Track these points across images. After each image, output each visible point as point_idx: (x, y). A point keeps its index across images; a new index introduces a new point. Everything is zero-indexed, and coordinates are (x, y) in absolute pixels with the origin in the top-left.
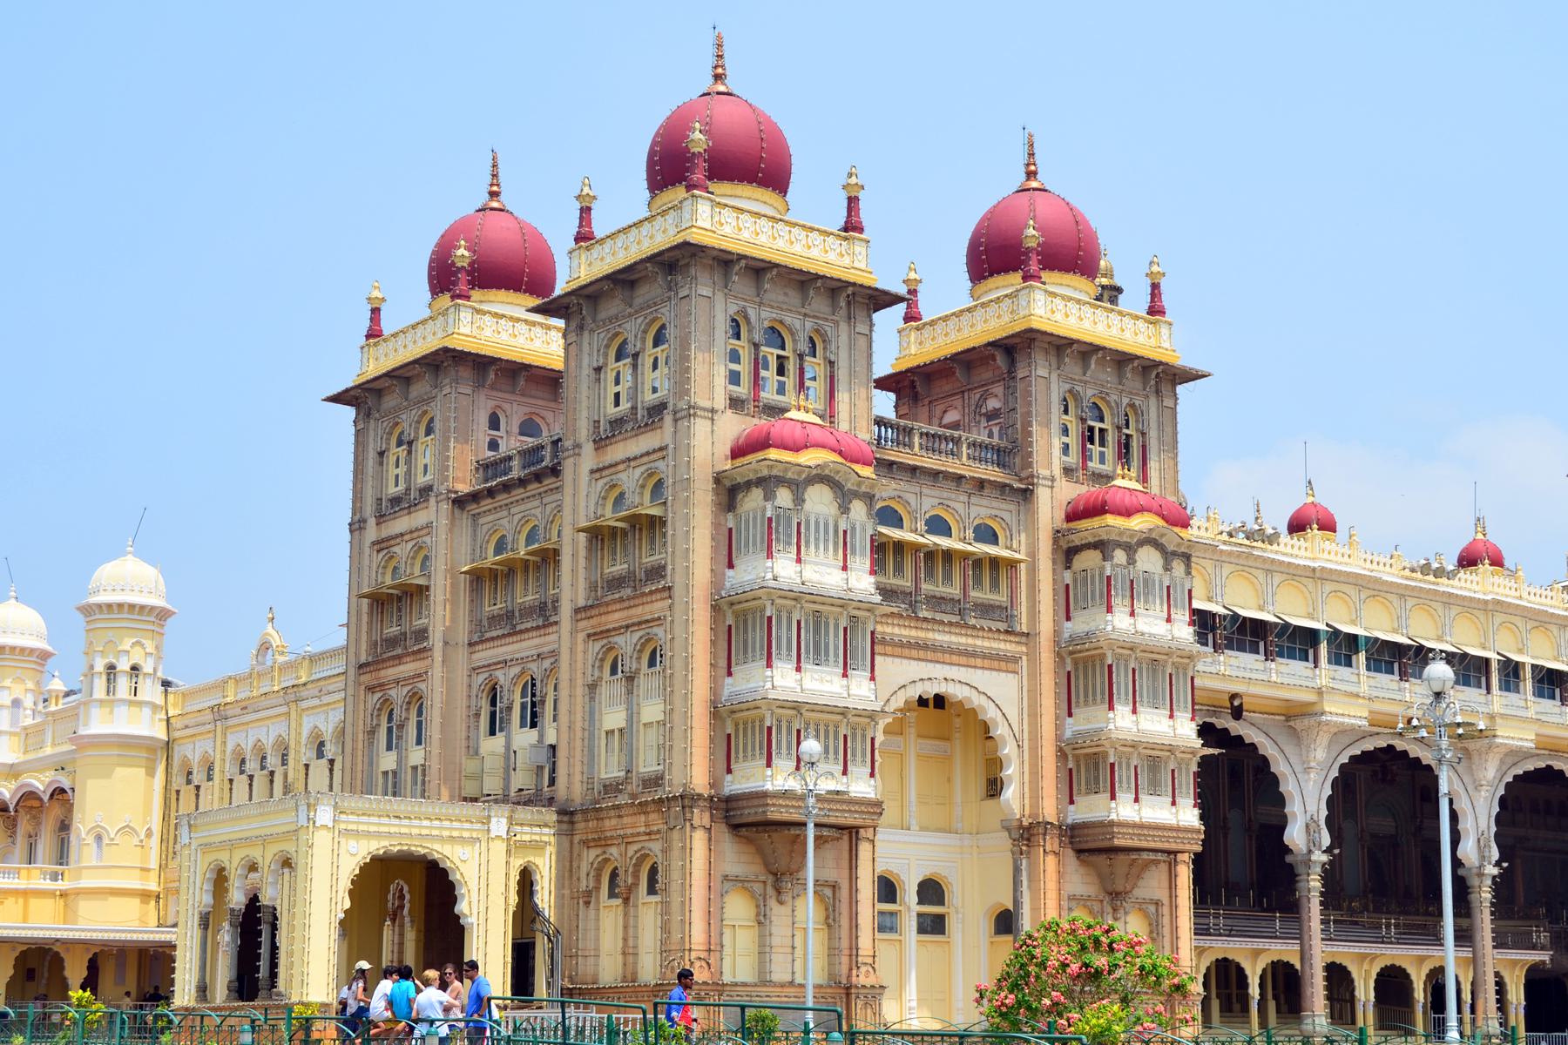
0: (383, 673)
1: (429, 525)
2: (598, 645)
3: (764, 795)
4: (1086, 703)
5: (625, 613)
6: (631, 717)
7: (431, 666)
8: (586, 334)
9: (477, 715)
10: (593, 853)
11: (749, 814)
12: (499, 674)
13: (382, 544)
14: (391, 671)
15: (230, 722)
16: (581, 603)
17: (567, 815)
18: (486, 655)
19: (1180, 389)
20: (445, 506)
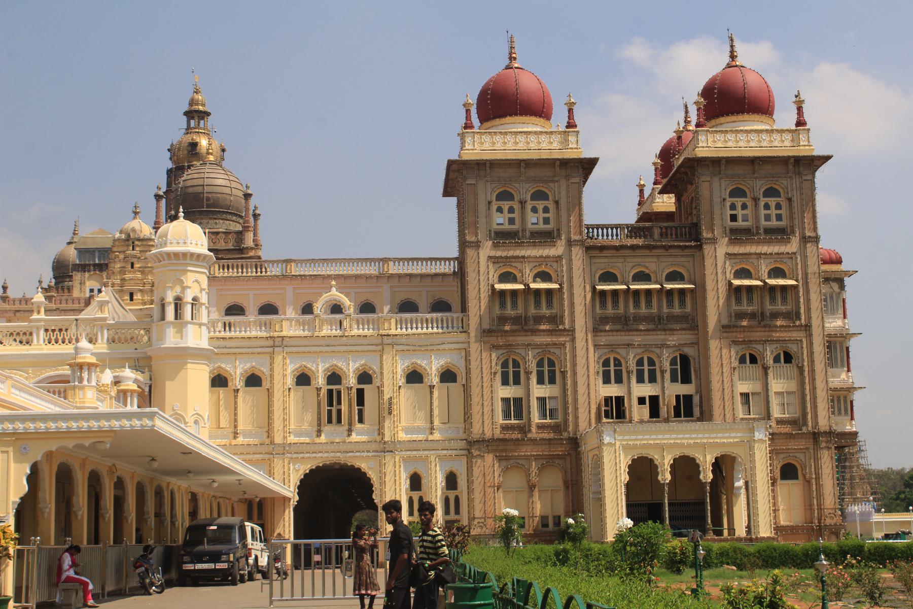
0: (511, 338)
5: (766, 334)
7: (573, 340)
14: (519, 338)
18: (603, 340)
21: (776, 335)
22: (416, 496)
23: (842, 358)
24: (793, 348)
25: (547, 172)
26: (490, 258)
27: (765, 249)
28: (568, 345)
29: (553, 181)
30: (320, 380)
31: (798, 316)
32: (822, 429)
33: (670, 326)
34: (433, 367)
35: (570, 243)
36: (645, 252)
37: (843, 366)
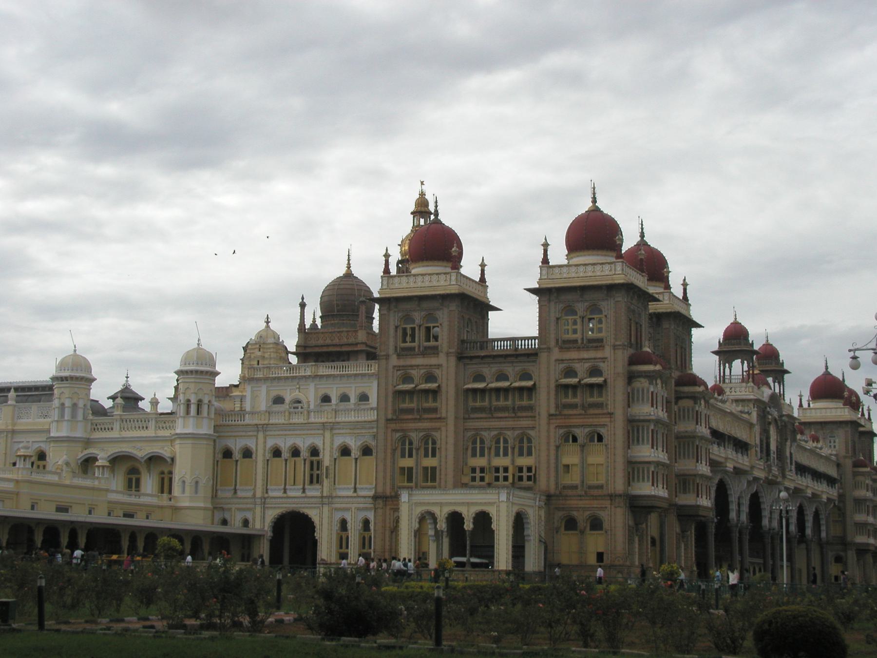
1: (439, 366)
2: (562, 431)
3: (654, 496)
4: (684, 458)
6: (583, 461)
8: (552, 304)
9: (467, 449)
10: (560, 514)
11: (644, 503)
12: (485, 434)
13: (398, 368)
15: (268, 433)
16: (552, 411)
17: (549, 497)
18: (471, 424)
19: (694, 331)
20: (453, 360)
21: (590, 421)
22: (344, 535)
23: (648, 437)
24: (602, 431)
25: (436, 304)
26: (394, 367)
27: (585, 355)
28: (443, 429)
29: (438, 309)
30: (305, 454)
31: (607, 405)
32: (617, 493)
33: (519, 414)
34: (355, 444)
35: (448, 354)
36: (501, 360)
37: (648, 443)
